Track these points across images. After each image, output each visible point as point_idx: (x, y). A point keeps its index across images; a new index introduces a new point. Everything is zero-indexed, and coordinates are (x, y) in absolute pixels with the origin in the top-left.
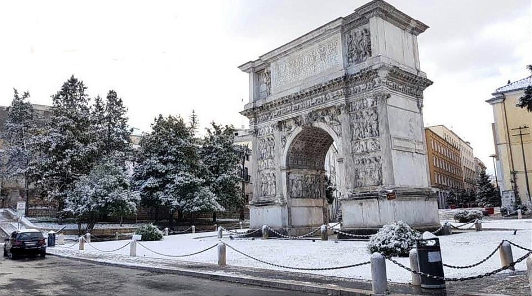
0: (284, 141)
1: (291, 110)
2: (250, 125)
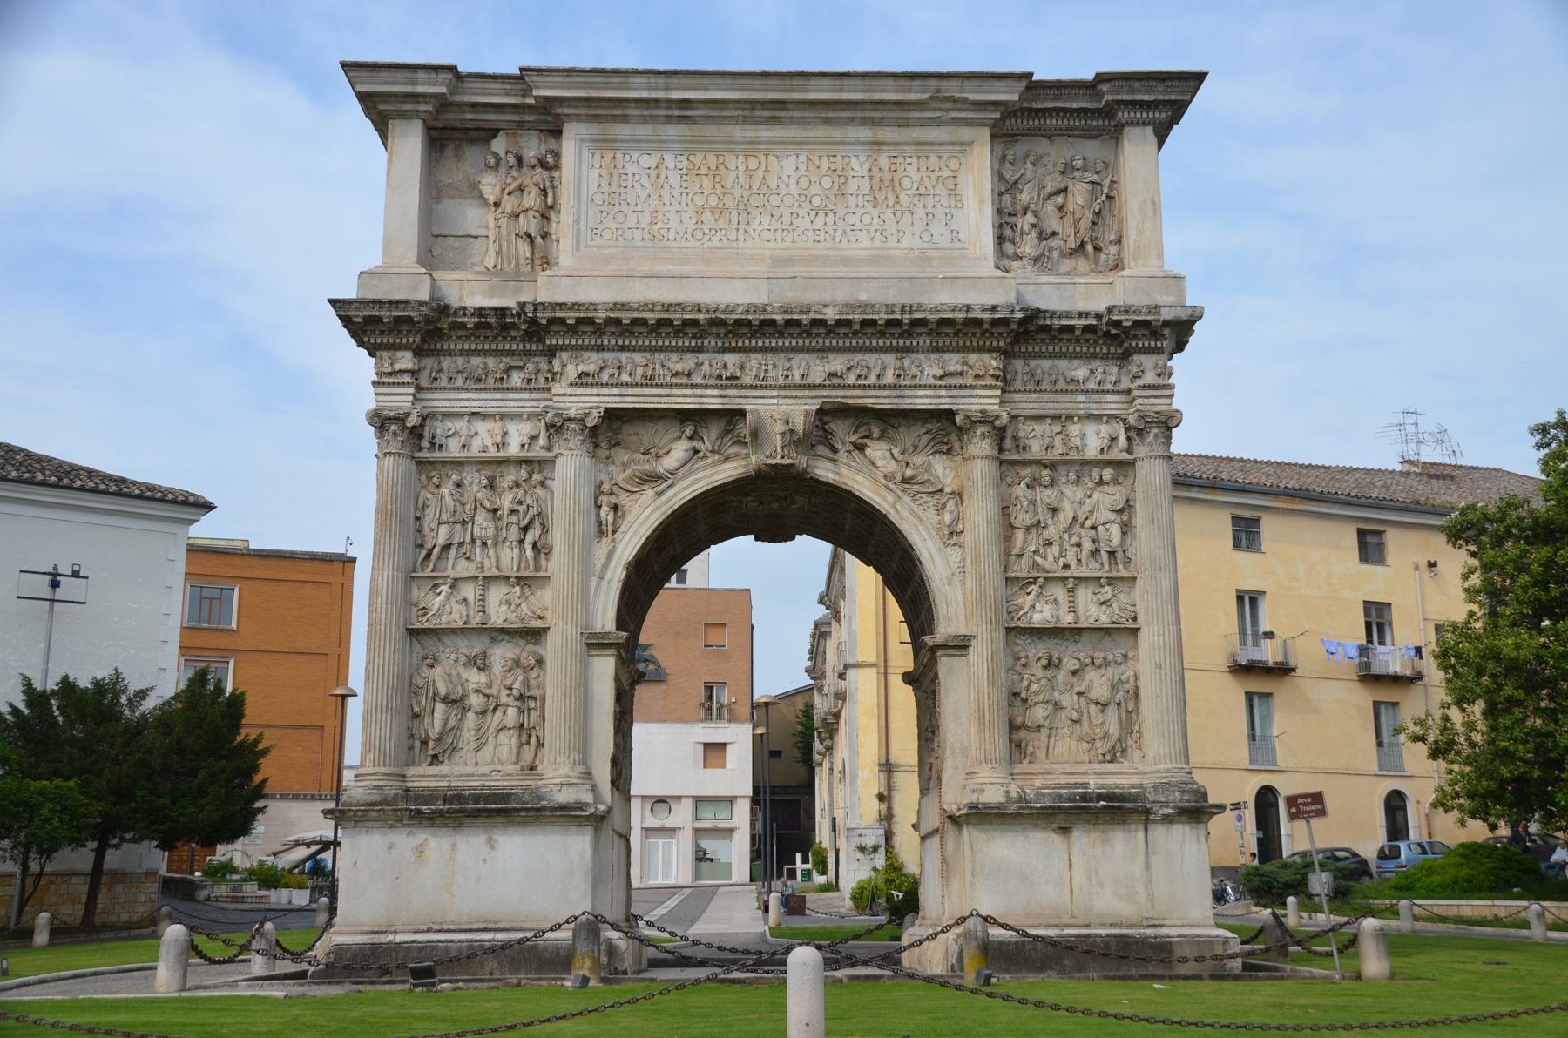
0: (615, 508)
1: (689, 375)
2: (374, 383)
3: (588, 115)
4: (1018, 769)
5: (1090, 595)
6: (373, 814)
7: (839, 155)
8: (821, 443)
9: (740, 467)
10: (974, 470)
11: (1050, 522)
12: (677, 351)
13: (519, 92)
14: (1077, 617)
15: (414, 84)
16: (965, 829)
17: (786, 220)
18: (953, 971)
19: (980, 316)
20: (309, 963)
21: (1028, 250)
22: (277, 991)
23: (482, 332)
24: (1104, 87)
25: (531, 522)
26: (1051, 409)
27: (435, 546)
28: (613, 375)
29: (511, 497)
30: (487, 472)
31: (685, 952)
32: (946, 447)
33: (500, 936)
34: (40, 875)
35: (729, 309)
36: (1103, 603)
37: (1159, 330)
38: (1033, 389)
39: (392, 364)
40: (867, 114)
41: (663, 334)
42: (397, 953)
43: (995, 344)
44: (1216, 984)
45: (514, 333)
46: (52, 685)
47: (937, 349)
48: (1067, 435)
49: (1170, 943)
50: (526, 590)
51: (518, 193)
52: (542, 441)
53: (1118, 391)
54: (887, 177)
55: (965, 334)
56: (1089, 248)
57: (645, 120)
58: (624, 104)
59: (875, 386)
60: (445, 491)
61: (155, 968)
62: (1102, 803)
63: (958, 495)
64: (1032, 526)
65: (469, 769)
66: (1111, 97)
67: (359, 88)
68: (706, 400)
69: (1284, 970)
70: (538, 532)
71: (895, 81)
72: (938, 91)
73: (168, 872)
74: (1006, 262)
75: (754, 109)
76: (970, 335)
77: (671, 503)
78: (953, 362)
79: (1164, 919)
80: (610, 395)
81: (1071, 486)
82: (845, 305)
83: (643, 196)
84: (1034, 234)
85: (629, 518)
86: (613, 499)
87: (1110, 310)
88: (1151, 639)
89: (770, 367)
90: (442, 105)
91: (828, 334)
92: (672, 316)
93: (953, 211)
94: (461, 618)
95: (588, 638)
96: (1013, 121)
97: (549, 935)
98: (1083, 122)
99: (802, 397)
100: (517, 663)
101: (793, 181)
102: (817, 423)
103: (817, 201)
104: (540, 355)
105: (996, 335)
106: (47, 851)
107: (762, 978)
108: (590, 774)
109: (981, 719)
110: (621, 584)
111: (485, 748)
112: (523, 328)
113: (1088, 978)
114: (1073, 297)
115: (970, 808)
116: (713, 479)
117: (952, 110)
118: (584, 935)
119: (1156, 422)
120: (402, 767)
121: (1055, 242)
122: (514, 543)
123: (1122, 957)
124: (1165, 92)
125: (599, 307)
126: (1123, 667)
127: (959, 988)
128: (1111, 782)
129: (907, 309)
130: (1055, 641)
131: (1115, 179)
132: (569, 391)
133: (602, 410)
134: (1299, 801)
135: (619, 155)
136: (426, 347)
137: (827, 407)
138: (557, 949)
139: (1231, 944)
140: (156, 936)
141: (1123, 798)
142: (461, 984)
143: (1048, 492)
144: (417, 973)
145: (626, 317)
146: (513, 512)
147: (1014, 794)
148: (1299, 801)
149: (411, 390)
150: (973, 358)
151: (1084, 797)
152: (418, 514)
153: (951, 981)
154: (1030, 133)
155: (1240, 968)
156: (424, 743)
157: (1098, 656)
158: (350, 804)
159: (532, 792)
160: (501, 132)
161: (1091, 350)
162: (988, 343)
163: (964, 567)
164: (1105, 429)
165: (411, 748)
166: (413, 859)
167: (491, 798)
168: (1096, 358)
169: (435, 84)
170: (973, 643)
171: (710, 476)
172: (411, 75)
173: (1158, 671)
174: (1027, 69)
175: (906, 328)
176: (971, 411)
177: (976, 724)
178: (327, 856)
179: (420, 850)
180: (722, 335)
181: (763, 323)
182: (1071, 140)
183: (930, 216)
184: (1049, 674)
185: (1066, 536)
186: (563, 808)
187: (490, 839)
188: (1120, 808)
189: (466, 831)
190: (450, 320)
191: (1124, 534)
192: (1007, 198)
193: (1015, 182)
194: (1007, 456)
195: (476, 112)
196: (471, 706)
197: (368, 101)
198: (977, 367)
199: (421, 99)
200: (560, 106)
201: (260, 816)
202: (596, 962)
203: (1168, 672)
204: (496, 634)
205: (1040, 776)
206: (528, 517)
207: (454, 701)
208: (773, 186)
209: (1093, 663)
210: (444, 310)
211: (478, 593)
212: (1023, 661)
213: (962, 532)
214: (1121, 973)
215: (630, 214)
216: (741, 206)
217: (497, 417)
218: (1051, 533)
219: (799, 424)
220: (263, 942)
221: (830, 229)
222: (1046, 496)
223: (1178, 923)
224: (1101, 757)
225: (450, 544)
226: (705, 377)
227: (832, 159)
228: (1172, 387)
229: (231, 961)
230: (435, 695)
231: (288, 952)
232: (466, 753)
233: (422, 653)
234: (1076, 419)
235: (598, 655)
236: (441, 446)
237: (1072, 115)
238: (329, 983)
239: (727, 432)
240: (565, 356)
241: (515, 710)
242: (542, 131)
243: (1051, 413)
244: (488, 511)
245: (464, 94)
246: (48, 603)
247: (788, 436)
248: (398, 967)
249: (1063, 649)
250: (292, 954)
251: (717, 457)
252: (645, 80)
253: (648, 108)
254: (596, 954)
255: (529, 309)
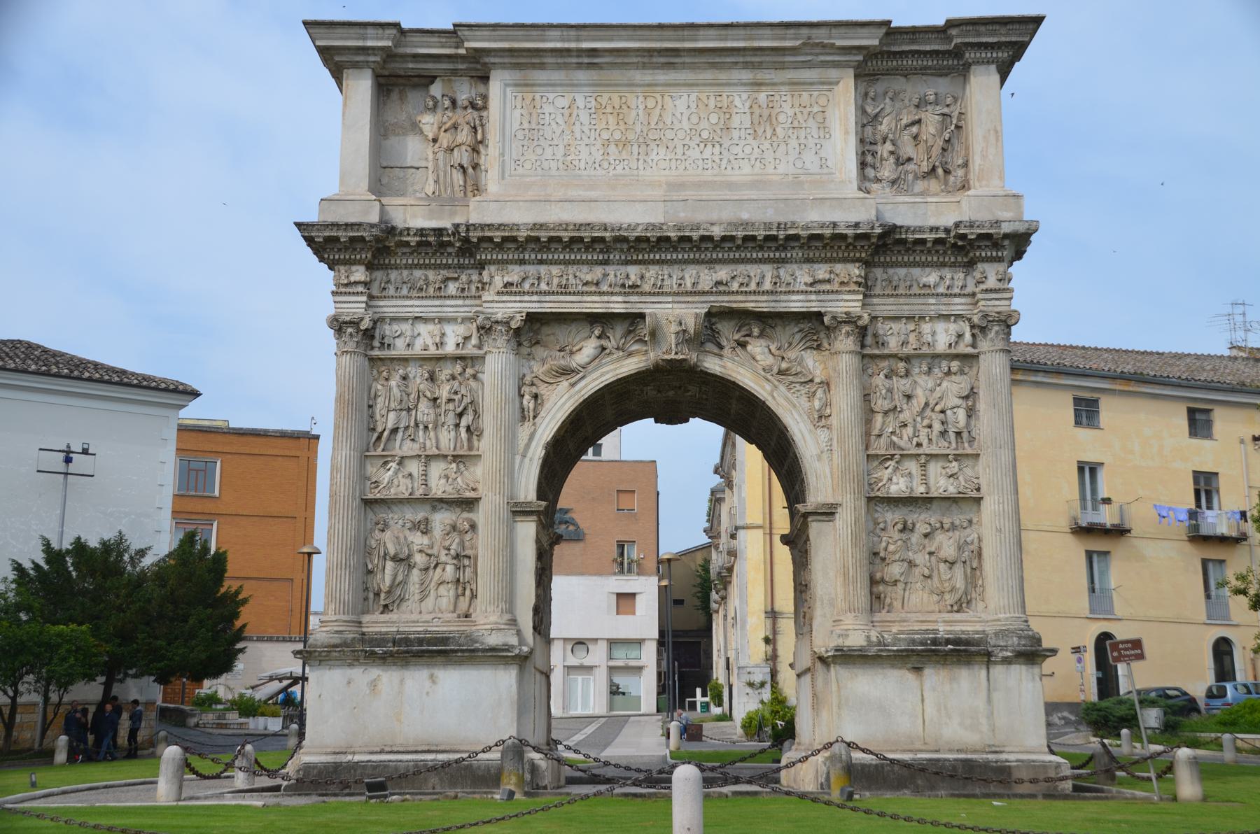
0: (536, 397)
1: (597, 284)
2: (333, 293)
3: (511, 64)
4: (877, 617)
5: (939, 470)
6: (335, 654)
7: (724, 94)
8: (709, 341)
9: (640, 362)
10: (841, 364)
11: (905, 407)
12: (588, 264)
13: (455, 45)
14: (928, 488)
15: (364, 38)
16: (832, 669)
17: (680, 150)
18: (822, 788)
19: (844, 232)
20: (283, 779)
21: (887, 174)
22: (256, 801)
23: (423, 249)
24: (954, 32)
25: (465, 409)
26: (906, 310)
27: (385, 430)
28: (533, 284)
29: (448, 388)
30: (428, 367)
31: (595, 771)
32: (816, 344)
33: (441, 757)
34: (59, 704)
35: (631, 228)
36: (951, 476)
37: (1000, 242)
38: (890, 293)
39: (348, 277)
40: (749, 59)
41: (575, 250)
42: (355, 771)
43: (858, 255)
44: (1048, 803)
45: (450, 250)
46: (67, 545)
47: (808, 260)
48: (920, 333)
49: (1009, 767)
50: (461, 466)
51: (453, 130)
52: (474, 341)
53: (964, 295)
54: (766, 113)
55: (832, 247)
56: (940, 171)
57: (559, 67)
58: (541, 54)
59: (755, 292)
60: (393, 383)
61: (156, 783)
62: (950, 647)
63: (826, 384)
64: (890, 410)
65: (414, 617)
66: (959, 40)
67: (318, 43)
68: (612, 305)
69: (1110, 791)
70: (471, 418)
71: (772, 30)
72: (809, 38)
73: (163, 702)
74: (867, 184)
75: (651, 56)
76: (836, 248)
77: (583, 392)
78: (822, 271)
79: (1004, 746)
80: (530, 302)
81: (923, 376)
82: (730, 224)
83: (558, 132)
84: (892, 160)
85: (547, 406)
86: (534, 390)
87: (957, 225)
88: (993, 508)
89: (666, 277)
90: (388, 56)
91: (714, 248)
92: (582, 235)
93: (823, 141)
94: (407, 489)
95: (513, 507)
96: (874, 62)
97: (481, 756)
98: (935, 62)
99: (693, 302)
100: (454, 528)
101: (685, 118)
102: (706, 324)
103: (705, 135)
104: (472, 268)
105: (859, 247)
106: (64, 686)
107: (660, 793)
108: (515, 621)
109: (845, 574)
110: (541, 461)
111: (427, 599)
112: (458, 245)
113: (937, 796)
114: (925, 214)
115: (836, 650)
116: (618, 372)
117: (822, 54)
118: (510, 756)
119: (997, 321)
120: (358, 615)
121: (910, 167)
122: (451, 427)
123: (966, 778)
124: (1007, 35)
125: (521, 227)
126: (968, 530)
127: (828, 803)
128: (957, 628)
129: (783, 226)
130: (910, 508)
131: (963, 111)
132: (496, 298)
133: (524, 314)
134: (1121, 646)
135: (538, 96)
136: (376, 262)
137: (714, 310)
138: (488, 768)
139: (1063, 768)
140: (155, 757)
141: (968, 642)
142: (408, 796)
143: (903, 381)
144: (372, 787)
145: (544, 235)
146: (450, 400)
147: (874, 639)
148: (1121, 646)
149: (364, 298)
150: (839, 267)
151: (935, 642)
152: (371, 403)
153: (820, 796)
154: (889, 73)
155: (1071, 789)
156: (377, 595)
157: (947, 521)
158: (316, 646)
159: (466, 637)
160: (438, 79)
161: (941, 259)
162: (852, 255)
163: (831, 445)
164: (953, 327)
165: (366, 599)
166: (368, 692)
167: (431, 641)
168: (945, 266)
169: (382, 39)
170: (839, 510)
171: (615, 369)
172: (362, 31)
173: (998, 534)
174: (887, 18)
175: (781, 242)
176: (837, 312)
177: (842, 579)
178: (296, 689)
179: (373, 685)
180: (625, 250)
181: (660, 239)
182: (924, 78)
183: (803, 146)
184: (904, 536)
185: (919, 419)
186: (493, 649)
187: (432, 676)
188: (965, 651)
189: (412, 668)
190: (396, 239)
191: (969, 417)
192: (869, 129)
193: (876, 116)
194: (868, 351)
195: (416, 62)
196: (415, 564)
197: (326, 54)
198: (842, 275)
199: (370, 52)
200: (488, 56)
201: (240, 656)
202: (521, 780)
203: (1007, 535)
204: (436, 503)
205: (897, 624)
206: (463, 405)
207: (402, 560)
208: (669, 122)
209: (942, 527)
210: (391, 231)
211: (421, 469)
212: (882, 526)
213: (830, 416)
214: (966, 792)
215: (546, 146)
216: (641, 140)
217: (436, 321)
218: (906, 416)
219: (691, 325)
220: (245, 761)
221: (717, 158)
222: (901, 384)
223: (1017, 750)
224: (949, 608)
225: (398, 428)
226: (610, 286)
227: (718, 99)
228: (1010, 290)
229: (218, 777)
230: (385, 554)
231: (265, 770)
232: (411, 604)
233: (375, 520)
234: (927, 318)
235: (522, 521)
236: (389, 345)
237: (925, 56)
238: (299, 795)
239: (630, 332)
240: (493, 268)
241: (453, 567)
242: (472, 77)
243: (906, 314)
244: (428, 398)
245: (406, 46)
246: (63, 475)
247: (681, 335)
248: (356, 782)
249: (916, 516)
250: (268, 771)
251: (621, 353)
252: (559, 33)
253: (561, 57)
254: (521, 772)
255: (462, 229)
